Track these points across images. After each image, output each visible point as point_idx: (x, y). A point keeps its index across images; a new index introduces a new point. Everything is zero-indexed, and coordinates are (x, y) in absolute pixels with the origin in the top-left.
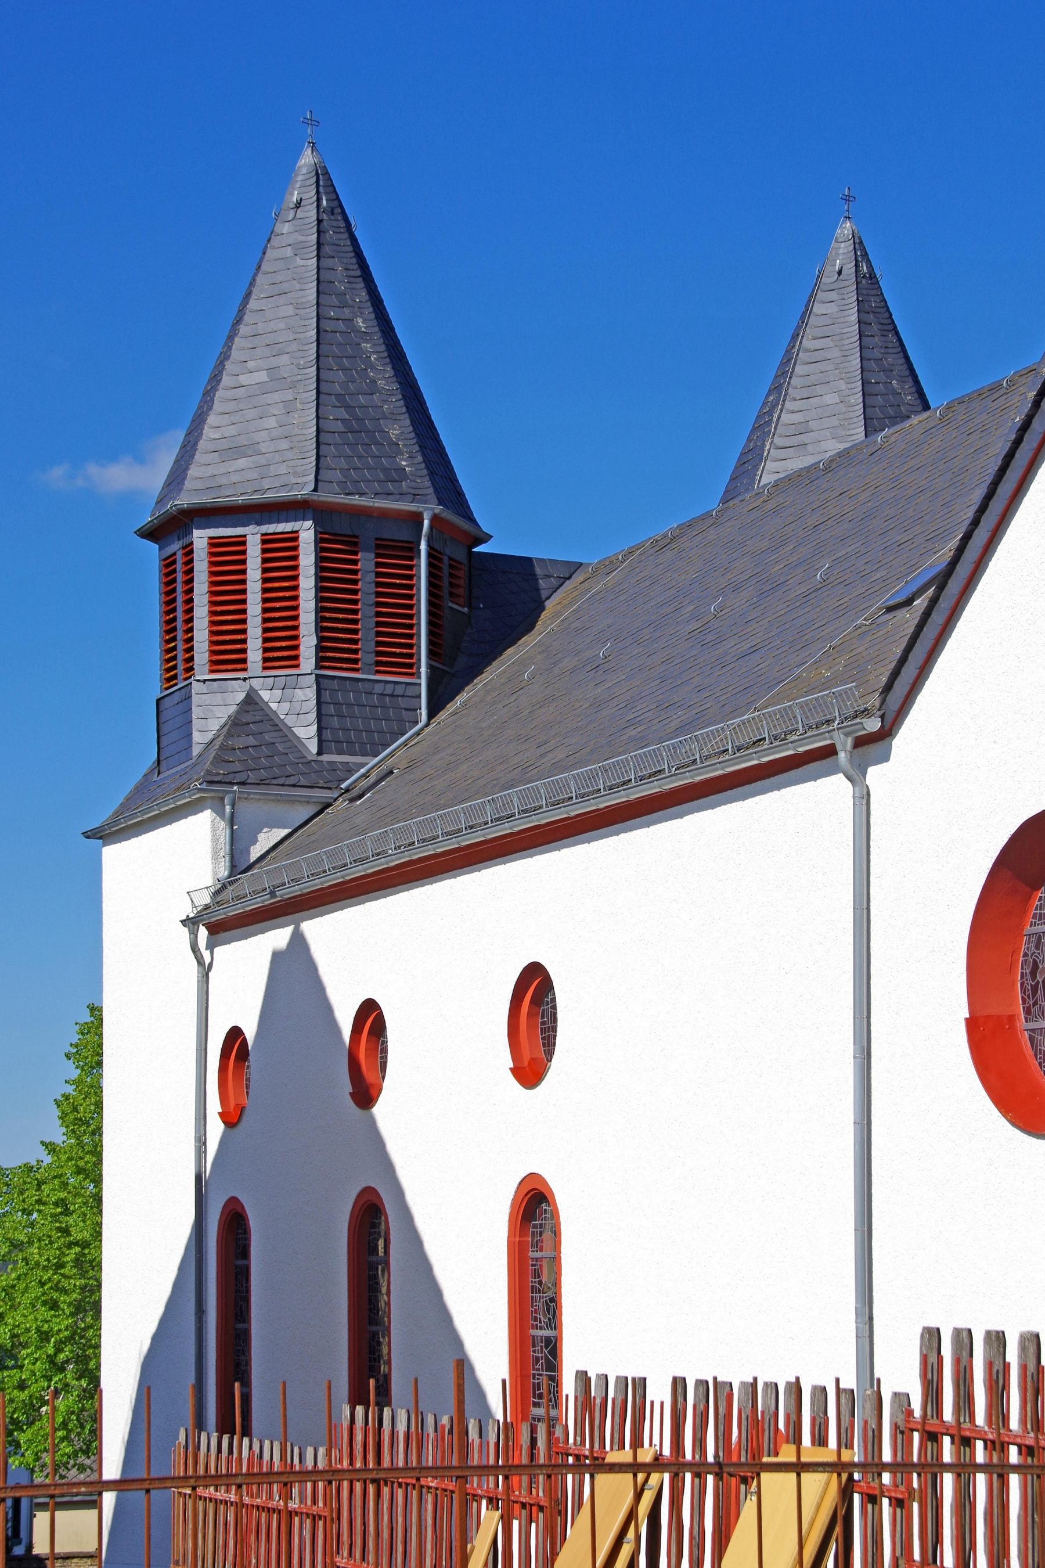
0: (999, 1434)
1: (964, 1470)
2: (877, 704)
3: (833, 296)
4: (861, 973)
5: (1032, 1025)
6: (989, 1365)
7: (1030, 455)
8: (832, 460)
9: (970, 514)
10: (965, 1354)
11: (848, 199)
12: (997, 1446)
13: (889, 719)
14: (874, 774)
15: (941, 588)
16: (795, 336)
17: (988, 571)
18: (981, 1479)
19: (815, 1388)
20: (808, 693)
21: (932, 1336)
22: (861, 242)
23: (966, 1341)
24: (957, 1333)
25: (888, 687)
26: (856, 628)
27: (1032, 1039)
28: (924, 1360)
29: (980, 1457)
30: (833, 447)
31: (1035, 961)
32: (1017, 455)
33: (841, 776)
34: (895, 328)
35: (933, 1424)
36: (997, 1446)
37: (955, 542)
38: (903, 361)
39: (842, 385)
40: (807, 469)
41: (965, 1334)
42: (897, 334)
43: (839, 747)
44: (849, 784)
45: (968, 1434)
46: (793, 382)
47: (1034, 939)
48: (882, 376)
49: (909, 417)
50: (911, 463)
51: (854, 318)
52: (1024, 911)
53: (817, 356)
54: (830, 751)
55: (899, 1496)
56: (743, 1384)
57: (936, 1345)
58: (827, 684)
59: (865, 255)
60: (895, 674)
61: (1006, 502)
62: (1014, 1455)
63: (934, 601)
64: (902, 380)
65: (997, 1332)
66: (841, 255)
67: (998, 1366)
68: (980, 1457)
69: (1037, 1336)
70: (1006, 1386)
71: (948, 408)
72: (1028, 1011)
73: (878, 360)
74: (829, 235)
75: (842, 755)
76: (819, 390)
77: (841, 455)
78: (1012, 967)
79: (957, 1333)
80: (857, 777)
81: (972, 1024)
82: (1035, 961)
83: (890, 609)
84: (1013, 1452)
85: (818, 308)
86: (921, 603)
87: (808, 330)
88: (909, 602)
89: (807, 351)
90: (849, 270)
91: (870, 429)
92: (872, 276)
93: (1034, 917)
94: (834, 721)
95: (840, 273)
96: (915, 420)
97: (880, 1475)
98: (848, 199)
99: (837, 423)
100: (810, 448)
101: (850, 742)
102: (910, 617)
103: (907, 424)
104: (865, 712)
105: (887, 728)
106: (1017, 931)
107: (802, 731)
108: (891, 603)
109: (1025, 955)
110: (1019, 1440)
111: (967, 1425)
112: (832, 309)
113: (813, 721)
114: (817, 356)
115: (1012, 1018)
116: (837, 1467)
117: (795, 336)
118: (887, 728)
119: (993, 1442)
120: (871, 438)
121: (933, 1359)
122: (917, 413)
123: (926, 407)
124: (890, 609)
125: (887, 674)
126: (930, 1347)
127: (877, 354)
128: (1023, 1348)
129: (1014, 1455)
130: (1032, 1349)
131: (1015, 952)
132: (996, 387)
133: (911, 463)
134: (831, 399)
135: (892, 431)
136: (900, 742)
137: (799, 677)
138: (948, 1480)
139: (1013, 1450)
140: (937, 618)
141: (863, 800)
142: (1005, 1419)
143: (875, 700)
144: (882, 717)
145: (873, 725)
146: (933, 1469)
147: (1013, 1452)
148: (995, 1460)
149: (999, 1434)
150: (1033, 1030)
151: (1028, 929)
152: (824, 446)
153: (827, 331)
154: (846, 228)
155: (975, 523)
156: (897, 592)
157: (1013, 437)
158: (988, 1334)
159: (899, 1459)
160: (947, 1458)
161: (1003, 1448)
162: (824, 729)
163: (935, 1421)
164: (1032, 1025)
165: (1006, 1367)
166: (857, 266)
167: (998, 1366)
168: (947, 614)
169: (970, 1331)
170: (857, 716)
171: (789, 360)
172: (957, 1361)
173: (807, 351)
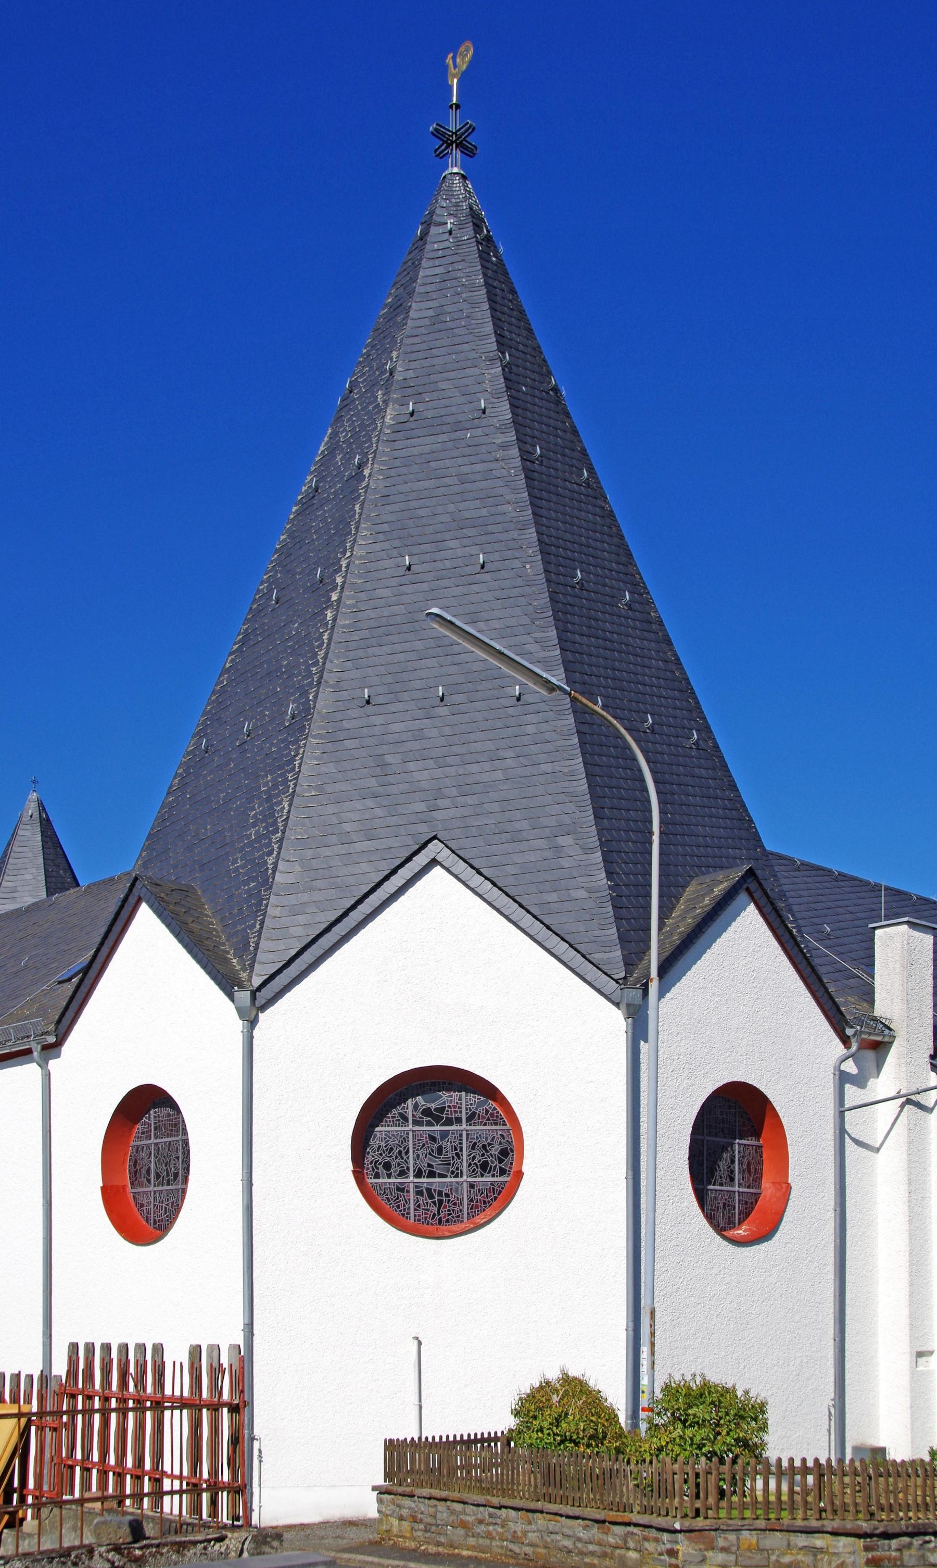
0: (123, 1395)
1: (88, 1412)
2: (54, 1029)
3: (28, 827)
4: (46, 1163)
5: (134, 1190)
6: (103, 1360)
7: (128, 914)
8: (29, 907)
9: (99, 939)
10: (91, 1355)
11: (35, 782)
12: (106, 1399)
13: (60, 1037)
14: (53, 1064)
15: (85, 974)
16: (9, 844)
17: (109, 968)
18: (113, 1416)
19: (27, 1376)
20: (17, 1022)
21: (74, 1347)
22: (42, 803)
23: (92, 1348)
24: (87, 1345)
25: (59, 1022)
26: (43, 991)
27: (134, 1197)
28: (70, 1358)
29: (97, 1405)
30: (29, 900)
31: (136, 1160)
32: (122, 913)
33: (35, 1064)
34: (61, 846)
35: (89, 1391)
36: (106, 1399)
37: (92, 952)
38: (65, 862)
39: (34, 870)
40: (16, 910)
41: (91, 1345)
42: (62, 848)
43: (34, 1049)
44: (39, 1068)
45: (91, 1394)
46: (8, 866)
47: (135, 1148)
48: (55, 868)
49: (69, 889)
50: (70, 912)
51: (40, 838)
52: (130, 1134)
53: (21, 855)
54: (29, 1052)
55: (55, 1426)
56: (12, 1375)
57: (76, 1351)
58: (27, 1018)
59: (44, 809)
60: (63, 1015)
61: (117, 935)
62: (114, 1403)
63: (81, 981)
64: (65, 871)
65: (107, 1344)
66: (31, 808)
67: (107, 1360)
68: (97, 1405)
69: (127, 1345)
70: (110, 1371)
71: (89, 886)
72: (132, 1183)
73: (52, 860)
74: (25, 798)
75: (35, 1054)
76: (22, 872)
77: (33, 904)
78: (124, 1161)
79: (87, 1345)
80: (43, 1064)
81: (104, 1190)
82: (136, 1160)
83: (60, 982)
84: (131, 1402)
85: (20, 832)
86: (75, 980)
87: (15, 842)
88: (70, 979)
89: (15, 852)
90: (36, 815)
91: (50, 892)
92: (48, 820)
93: (135, 1137)
94: (31, 1036)
95: (31, 816)
96: (72, 891)
97: (62, 1417)
98: (35, 782)
99: (32, 889)
100: (18, 900)
101: (39, 1047)
102: (69, 988)
103: (68, 893)
104: (47, 1033)
105: (59, 1041)
106: (127, 1144)
107: (14, 1040)
108: (60, 979)
109: (131, 1156)
110: (116, 1396)
111: (91, 1389)
112: (28, 833)
113: (20, 1036)
114: (21, 855)
115: (124, 1187)
116: (19, 1415)
117: (9, 844)
118: (59, 1041)
119: (120, 1399)
120: (50, 898)
121: (74, 1357)
122: (73, 887)
123: (78, 885)
124: (60, 982)
125: (59, 1014)
126: (73, 1352)
127: (51, 857)
128: (120, 1351)
129: (114, 1403)
130: (124, 1351)
131: (126, 1154)
132: (112, 879)
133: (70, 912)
134: (28, 877)
135: (60, 895)
136: (66, 1048)
137: (12, 1013)
138: (97, 1417)
139: (114, 1400)
140: (84, 989)
141: (47, 1078)
142: (110, 1384)
143: (52, 1027)
144: (56, 1036)
145: (52, 1039)
146: (73, 1413)
147: (131, 1402)
148: (121, 1406)
149: (123, 1395)
150: (135, 1193)
151: (132, 1143)
152: (25, 899)
153: (25, 843)
154: (34, 796)
155: (102, 944)
156: (64, 974)
157: (120, 904)
158: (103, 1345)
159: (55, 1409)
160: (80, 1407)
161: (125, 1401)
162: (26, 1040)
163: (75, 1388)
164: (134, 1190)
165: (111, 1360)
166: (40, 814)
167: (107, 1360)
168: (88, 987)
169: (93, 1344)
170: (42, 1035)
171: (6, 856)
172: (86, 1358)
173: (15, 852)
